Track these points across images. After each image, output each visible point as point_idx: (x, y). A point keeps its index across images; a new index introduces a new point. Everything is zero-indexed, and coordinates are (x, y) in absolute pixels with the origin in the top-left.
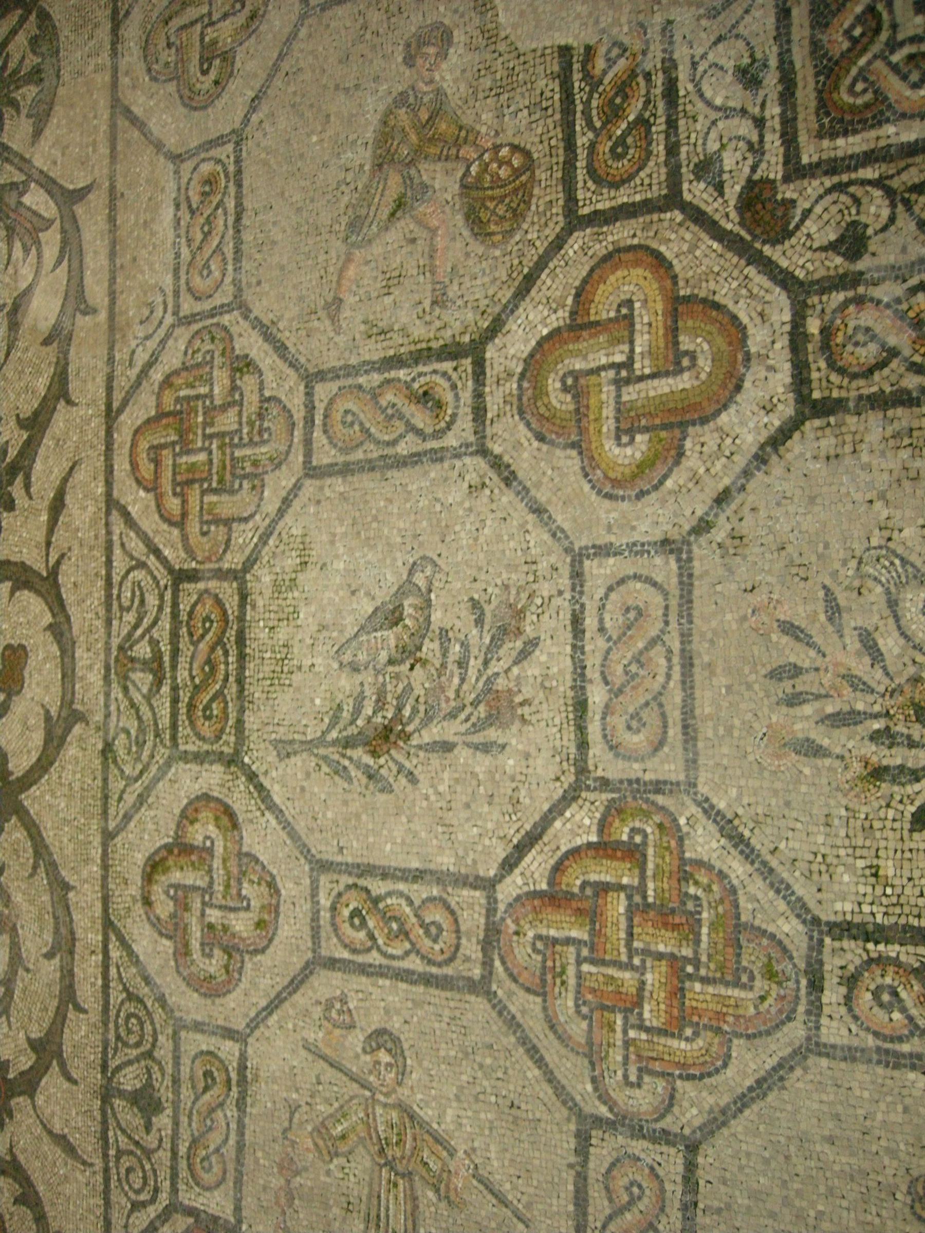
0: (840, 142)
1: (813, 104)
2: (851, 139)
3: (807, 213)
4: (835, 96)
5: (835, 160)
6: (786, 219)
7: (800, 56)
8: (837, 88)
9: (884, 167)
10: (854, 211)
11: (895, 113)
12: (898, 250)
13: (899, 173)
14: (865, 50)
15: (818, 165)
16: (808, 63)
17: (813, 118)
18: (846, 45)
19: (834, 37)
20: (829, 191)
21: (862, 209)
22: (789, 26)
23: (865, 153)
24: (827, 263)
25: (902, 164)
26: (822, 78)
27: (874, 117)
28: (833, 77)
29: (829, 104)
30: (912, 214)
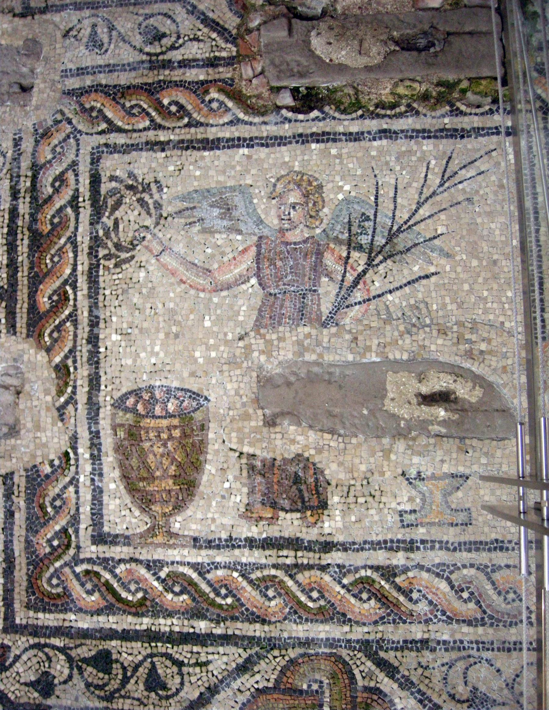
0: (40, 615)
1: (25, 584)
2: (47, 615)
3: (17, 658)
4: (39, 582)
5: (37, 626)
6: (4, 657)
7: (18, 548)
8: (40, 578)
9: (67, 641)
10: (47, 665)
11: (75, 606)
12: (73, 699)
13: (76, 647)
14: (59, 557)
15: (26, 627)
16: (23, 554)
17: (24, 593)
18: (48, 550)
19: (41, 541)
20: (32, 647)
21: (52, 664)
22: (13, 523)
23: (56, 627)
24: (29, 694)
25: (78, 642)
26: (31, 567)
27: (62, 605)
28: (38, 570)
29: (35, 587)
30: (82, 677)
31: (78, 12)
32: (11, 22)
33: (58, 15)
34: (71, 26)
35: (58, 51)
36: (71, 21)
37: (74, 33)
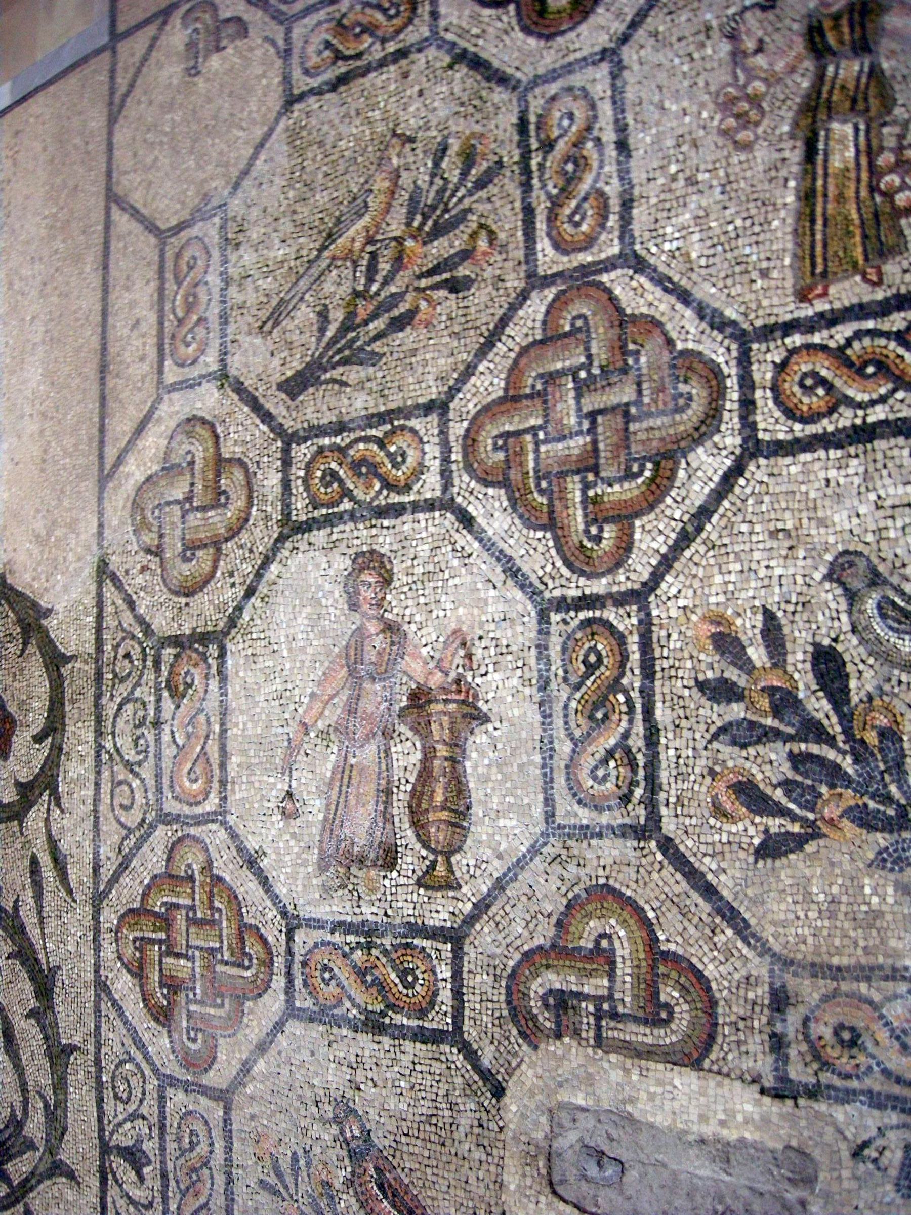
31: (876, 1112)
32: (757, 1103)
33: (840, 1108)
34: (866, 1137)
35: (846, 1184)
36: (866, 1128)
37: (871, 1152)
